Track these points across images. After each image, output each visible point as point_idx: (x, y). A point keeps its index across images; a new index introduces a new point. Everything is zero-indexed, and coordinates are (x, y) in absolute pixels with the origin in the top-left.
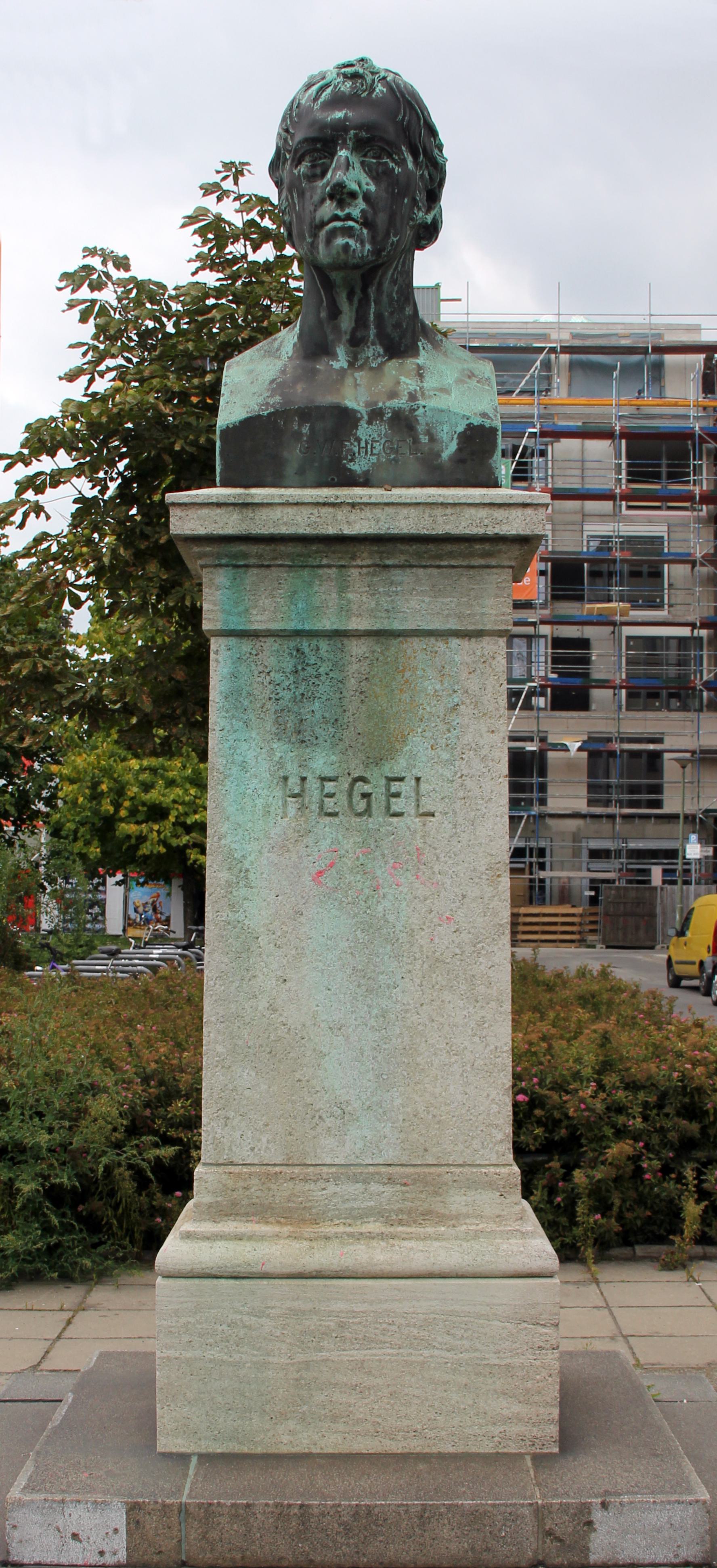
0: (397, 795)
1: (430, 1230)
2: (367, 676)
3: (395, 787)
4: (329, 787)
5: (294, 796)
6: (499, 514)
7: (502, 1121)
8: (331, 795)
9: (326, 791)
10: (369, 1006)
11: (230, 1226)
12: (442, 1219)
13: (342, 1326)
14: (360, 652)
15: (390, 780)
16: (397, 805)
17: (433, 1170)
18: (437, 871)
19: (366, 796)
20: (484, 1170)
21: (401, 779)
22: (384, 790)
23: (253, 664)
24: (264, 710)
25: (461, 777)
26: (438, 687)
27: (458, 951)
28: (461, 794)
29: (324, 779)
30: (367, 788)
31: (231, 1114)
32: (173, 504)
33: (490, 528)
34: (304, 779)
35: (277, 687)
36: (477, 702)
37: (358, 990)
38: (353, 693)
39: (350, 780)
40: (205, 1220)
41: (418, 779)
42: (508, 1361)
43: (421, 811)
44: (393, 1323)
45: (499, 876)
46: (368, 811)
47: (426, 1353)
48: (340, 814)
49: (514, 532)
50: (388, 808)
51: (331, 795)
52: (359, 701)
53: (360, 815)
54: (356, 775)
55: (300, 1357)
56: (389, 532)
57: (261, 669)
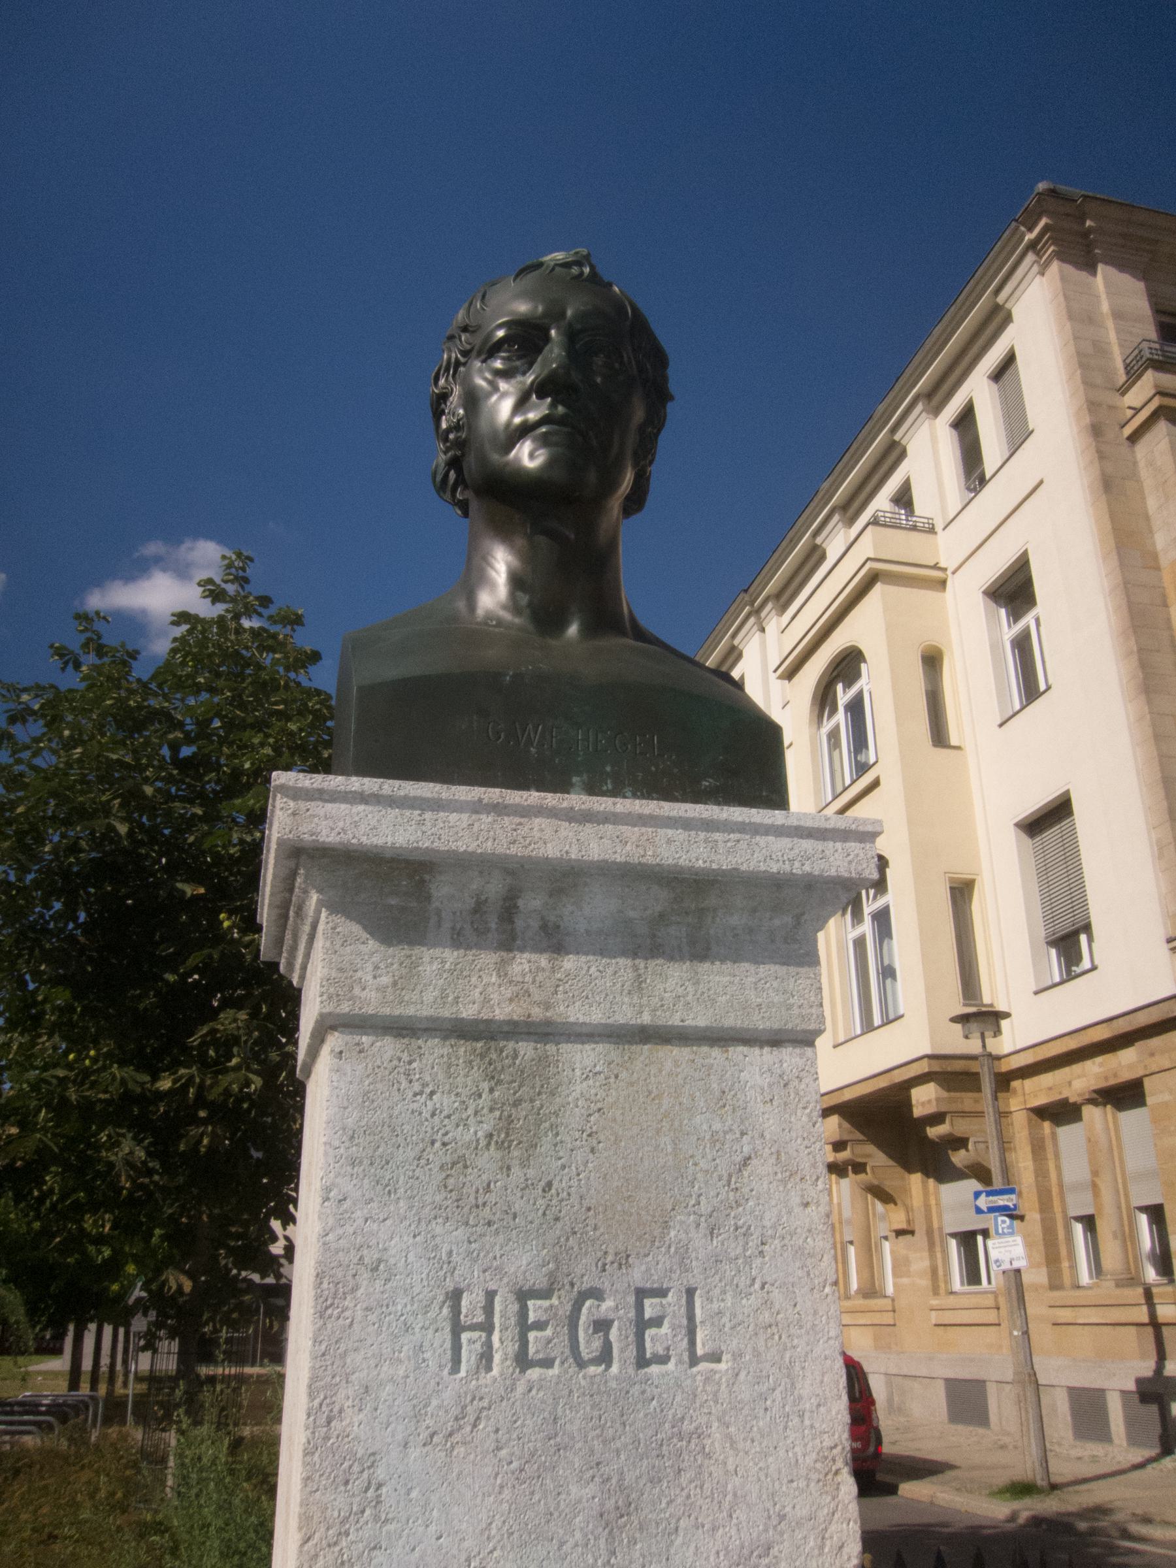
0: (657, 1322)
2: (599, 1105)
3: (651, 1308)
4: (535, 1309)
5: (473, 1328)
6: (807, 845)
14: (588, 1062)
15: (641, 1294)
18: (731, 1468)
19: (602, 1326)
21: (662, 1293)
23: (402, 1078)
24: (423, 1162)
26: (717, 1126)
28: (766, 1317)
32: (283, 789)
33: (797, 864)
34: (490, 1295)
35: (446, 1121)
36: (778, 1153)
38: (577, 1134)
41: (690, 1293)
45: (837, 1473)
46: (605, 1357)
48: (557, 1362)
49: (833, 873)
51: (540, 1326)
52: (588, 1149)
54: (585, 1286)
56: (643, 860)
57: (417, 1087)
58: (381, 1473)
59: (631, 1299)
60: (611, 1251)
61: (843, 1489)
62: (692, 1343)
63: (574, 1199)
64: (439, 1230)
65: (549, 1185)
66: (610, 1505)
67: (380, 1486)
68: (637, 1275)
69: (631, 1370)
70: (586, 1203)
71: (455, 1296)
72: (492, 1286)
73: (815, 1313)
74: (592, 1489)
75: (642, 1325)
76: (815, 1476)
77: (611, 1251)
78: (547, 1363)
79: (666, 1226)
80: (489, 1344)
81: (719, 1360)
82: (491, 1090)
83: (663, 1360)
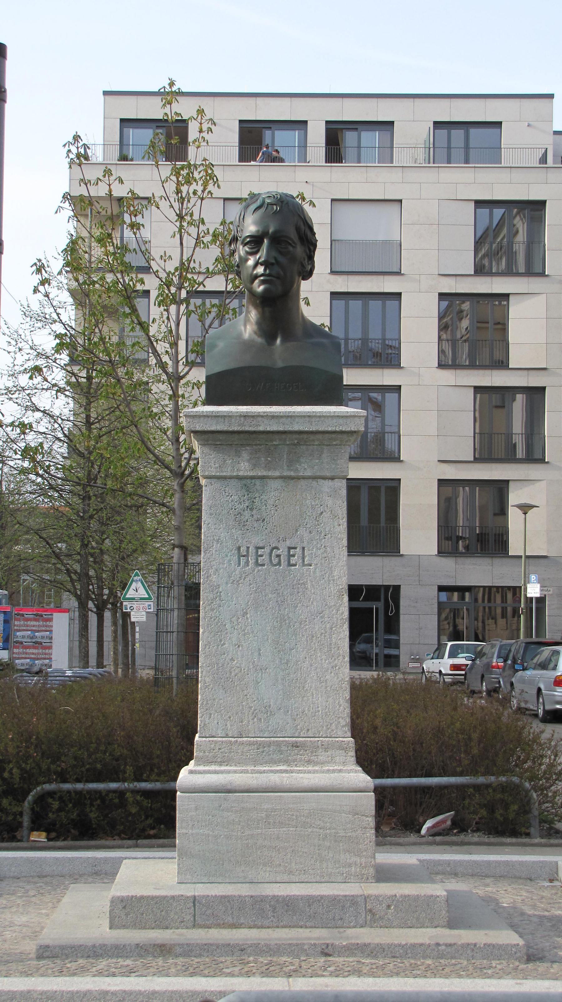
0: (294, 556)
1: (310, 768)
3: (292, 552)
5: (244, 556)
7: (345, 715)
8: (261, 556)
9: (259, 553)
10: (281, 659)
11: (213, 768)
12: (316, 763)
13: (267, 816)
15: (290, 548)
16: (293, 560)
17: (312, 739)
19: (278, 556)
20: (337, 739)
21: (295, 548)
22: (286, 553)
25: (325, 547)
26: (313, 503)
27: (323, 631)
29: (258, 548)
30: (279, 552)
31: (213, 712)
34: (248, 548)
37: (275, 651)
39: (271, 548)
40: (200, 765)
42: (350, 834)
43: (306, 563)
44: (293, 815)
45: (343, 595)
46: (279, 564)
47: (310, 830)
50: (289, 562)
51: (261, 556)
53: (276, 565)
55: (247, 832)
57: (227, 494)
58: (221, 590)
59: (286, 550)
60: (281, 537)
61: (344, 599)
62: (304, 561)
63: (271, 523)
64: (234, 531)
65: (264, 520)
66: (279, 599)
67: (221, 592)
68: (288, 543)
69: (286, 567)
70: (274, 524)
71: (239, 548)
72: (248, 546)
73: (340, 554)
74: (274, 595)
75: (290, 556)
76: (336, 595)
77: (281, 537)
78: (263, 565)
79: (297, 531)
80: (248, 560)
81: (311, 566)
82: (248, 494)
83: (295, 565)
